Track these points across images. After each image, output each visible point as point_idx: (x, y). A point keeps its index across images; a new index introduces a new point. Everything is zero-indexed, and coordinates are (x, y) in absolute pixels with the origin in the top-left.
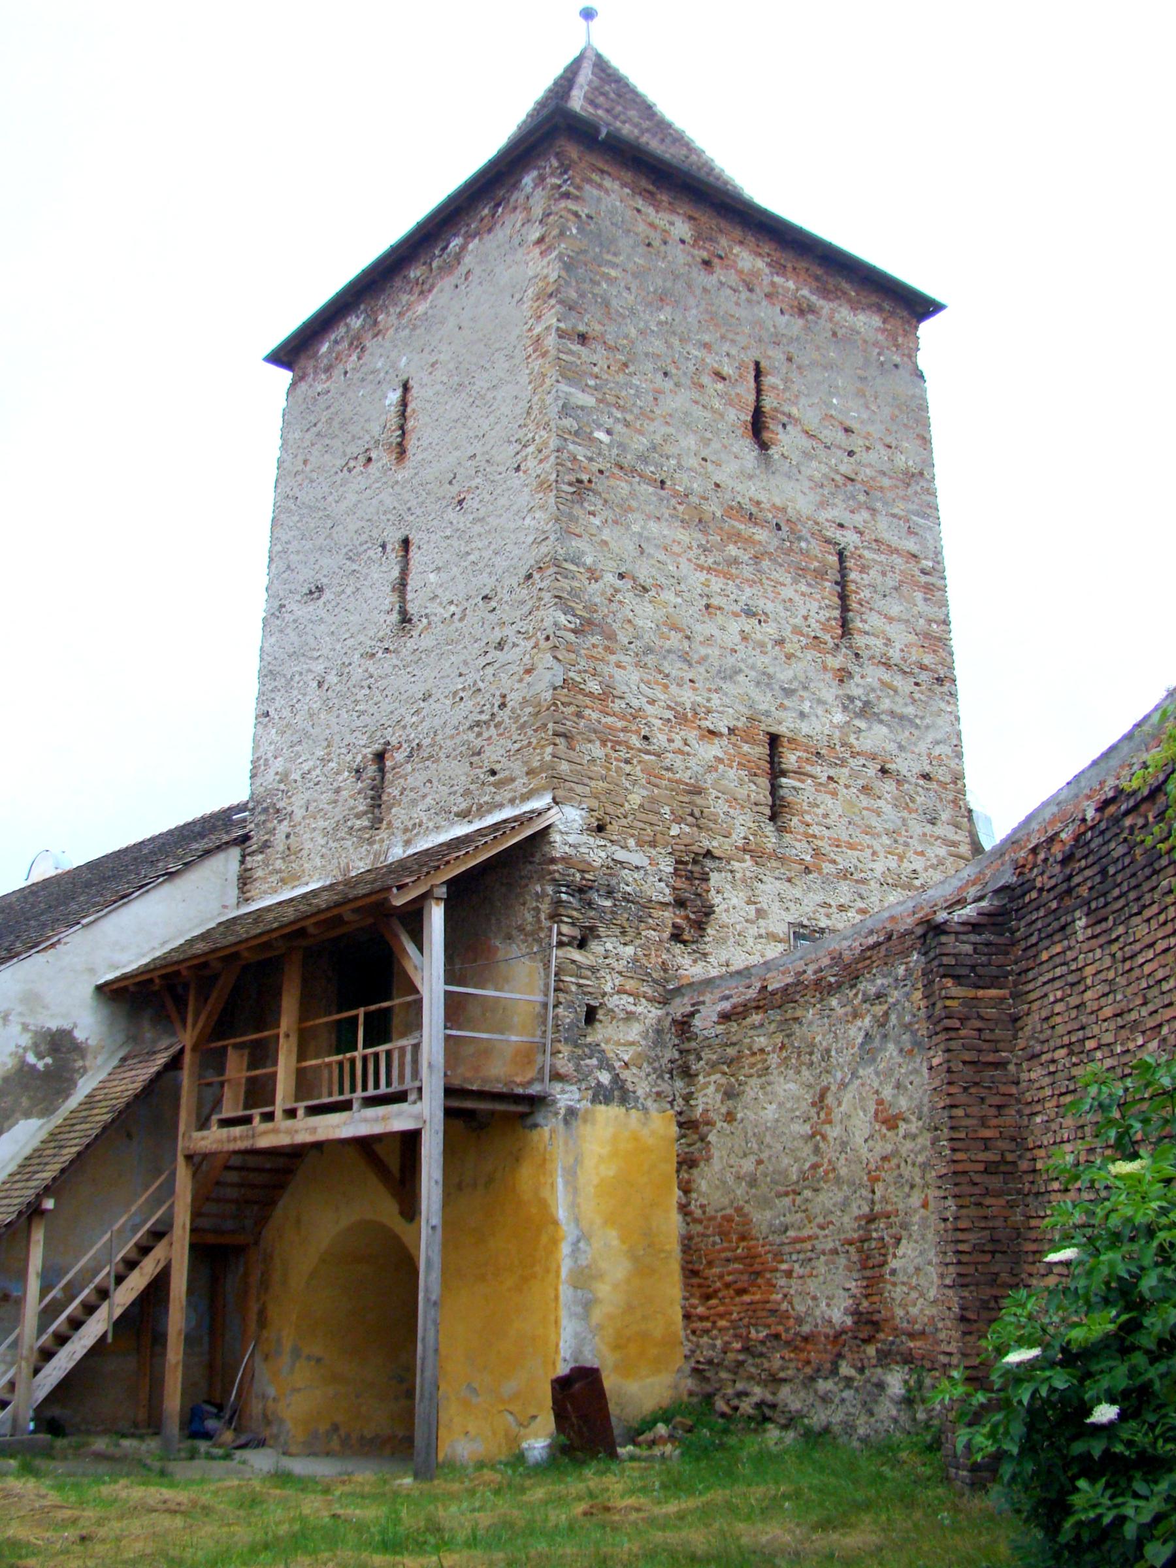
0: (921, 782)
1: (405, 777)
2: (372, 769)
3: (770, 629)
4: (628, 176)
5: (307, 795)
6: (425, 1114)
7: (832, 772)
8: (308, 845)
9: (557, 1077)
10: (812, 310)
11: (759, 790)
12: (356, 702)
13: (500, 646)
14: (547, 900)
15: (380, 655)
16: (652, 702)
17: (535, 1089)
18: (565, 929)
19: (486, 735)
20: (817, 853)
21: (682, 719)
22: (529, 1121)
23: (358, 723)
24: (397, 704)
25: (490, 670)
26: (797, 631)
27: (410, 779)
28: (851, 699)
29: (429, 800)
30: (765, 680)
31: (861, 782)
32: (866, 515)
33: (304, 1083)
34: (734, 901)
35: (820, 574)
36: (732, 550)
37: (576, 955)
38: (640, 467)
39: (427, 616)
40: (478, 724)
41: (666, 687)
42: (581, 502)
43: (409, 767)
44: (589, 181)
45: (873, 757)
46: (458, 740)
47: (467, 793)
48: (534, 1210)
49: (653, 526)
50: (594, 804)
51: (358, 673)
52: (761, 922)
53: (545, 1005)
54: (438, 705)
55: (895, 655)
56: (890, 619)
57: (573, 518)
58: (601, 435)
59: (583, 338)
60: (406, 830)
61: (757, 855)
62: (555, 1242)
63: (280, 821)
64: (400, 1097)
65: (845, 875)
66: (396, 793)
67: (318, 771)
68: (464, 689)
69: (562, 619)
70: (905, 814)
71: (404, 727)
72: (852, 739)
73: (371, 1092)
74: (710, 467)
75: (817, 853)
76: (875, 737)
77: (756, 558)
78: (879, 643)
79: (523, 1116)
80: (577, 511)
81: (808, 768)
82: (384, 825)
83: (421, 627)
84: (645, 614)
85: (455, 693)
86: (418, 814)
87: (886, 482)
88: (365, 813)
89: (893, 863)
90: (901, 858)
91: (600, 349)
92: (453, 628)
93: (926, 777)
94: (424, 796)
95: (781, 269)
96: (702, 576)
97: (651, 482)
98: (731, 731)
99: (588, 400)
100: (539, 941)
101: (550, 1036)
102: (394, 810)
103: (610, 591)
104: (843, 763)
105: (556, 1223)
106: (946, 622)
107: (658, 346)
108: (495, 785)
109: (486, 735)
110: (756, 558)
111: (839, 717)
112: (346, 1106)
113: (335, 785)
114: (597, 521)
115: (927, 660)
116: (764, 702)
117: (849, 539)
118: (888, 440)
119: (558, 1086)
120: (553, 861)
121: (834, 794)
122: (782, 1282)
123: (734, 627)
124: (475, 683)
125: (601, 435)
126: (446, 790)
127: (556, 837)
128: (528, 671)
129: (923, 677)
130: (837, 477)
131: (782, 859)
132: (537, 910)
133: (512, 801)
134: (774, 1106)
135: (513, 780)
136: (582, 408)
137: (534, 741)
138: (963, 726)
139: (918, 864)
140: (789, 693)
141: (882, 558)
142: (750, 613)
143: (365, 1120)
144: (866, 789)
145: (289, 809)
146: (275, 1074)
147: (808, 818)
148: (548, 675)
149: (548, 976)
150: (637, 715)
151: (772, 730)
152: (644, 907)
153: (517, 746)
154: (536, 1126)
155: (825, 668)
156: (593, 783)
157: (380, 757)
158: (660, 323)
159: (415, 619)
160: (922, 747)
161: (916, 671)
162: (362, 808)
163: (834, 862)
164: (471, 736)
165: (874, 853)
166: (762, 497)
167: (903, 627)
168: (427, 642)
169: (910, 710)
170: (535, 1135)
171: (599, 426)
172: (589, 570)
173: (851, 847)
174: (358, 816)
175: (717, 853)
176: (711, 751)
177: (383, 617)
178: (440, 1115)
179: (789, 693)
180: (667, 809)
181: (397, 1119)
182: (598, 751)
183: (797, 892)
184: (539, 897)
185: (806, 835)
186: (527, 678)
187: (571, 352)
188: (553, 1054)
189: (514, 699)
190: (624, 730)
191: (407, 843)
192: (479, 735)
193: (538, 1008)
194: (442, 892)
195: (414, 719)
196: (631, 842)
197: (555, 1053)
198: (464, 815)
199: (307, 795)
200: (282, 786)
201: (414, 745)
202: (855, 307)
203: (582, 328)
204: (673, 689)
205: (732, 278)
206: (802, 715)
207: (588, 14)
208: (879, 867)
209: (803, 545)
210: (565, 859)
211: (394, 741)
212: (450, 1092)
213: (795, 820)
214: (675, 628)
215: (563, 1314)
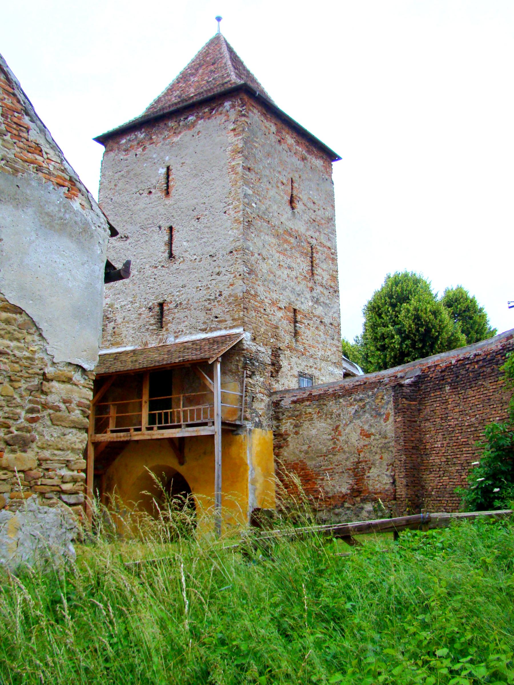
1: (174, 313)
2: (157, 309)
3: (294, 273)
4: (260, 108)
5: (124, 314)
6: (217, 429)
8: (125, 332)
9: (246, 419)
11: (290, 328)
12: (148, 283)
13: (218, 274)
14: (242, 362)
15: (160, 267)
16: (266, 298)
17: (238, 423)
18: (248, 372)
19: (213, 304)
20: (305, 349)
22: (235, 433)
23: (150, 291)
24: (169, 287)
25: (213, 282)
27: (177, 315)
28: (313, 297)
29: (186, 323)
30: (293, 291)
32: (318, 233)
33: (152, 420)
35: (306, 254)
36: (285, 246)
37: (250, 380)
38: (263, 216)
39: (182, 257)
40: (209, 300)
42: (250, 228)
43: (176, 310)
44: (250, 110)
46: (199, 304)
47: (204, 323)
48: (237, 461)
51: (149, 273)
53: (242, 396)
54: (189, 290)
55: (324, 282)
57: (248, 234)
58: (254, 205)
59: (249, 169)
60: (175, 332)
62: (246, 470)
63: (110, 322)
64: (205, 424)
65: (311, 356)
66: (170, 319)
67: (129, 306)
68: (201, 286)
69: (245, 269)
71: (173, 296)
73: (189, 422)
75: (305, 349)
78: (321, 278)
79: (233, 431)
82: (164, 329)
83: (180, 261)
85: (197, 288)
86: (181, 327)
87: (323, 222)
88: (155, 324)
91: (253, 173)
92: (196, 264)
94: (184, 322)
99: (250, 192)
100: (238, 375)
101: (243, 406)
102: (169, 325)
105: (247, 464)
106: (337, 272)
107: (267, 173)
108: (218, 322)
109: (213, 304)
111: (310, 304)
112: (179, 426)
113: (139, 312)
114: (253, 235)
117: (314, 242)
118: (324, 207)
119: (246, 422)
120: (244, 350)
121: (309, 329)
122: (320, 482)
124: (207, 285)
125: (254, 205)
126: (195, 321)
127: (244, 342)
128: (231, 285)
129: (331, 290)
132: (238, 365)
133: (225, 328)
134: (315, 430)
135: (226, 321)
136: (249, 195)
137: (235, 310)
138: (341, 307)
139: (329, 354)
142: (290, 268)
143: (188, 431)
145: (114, 318)
146: (141, 415)
148: (241, 288)
149: (243, 387)
153: (227, 310)
154: (238, 434)
156: (253, 325)
157: (161, 305)
158: (268, 164)
159: (177, 257)
162: (152, 322)
164: (206, 304)
168: (183, 266)
169: (328, 302)
170: (238, 437)
173: (313, 347)
174: (151, 325)
175: (281, 348)
176: (280, 314)
177: (160, 254)
178: (220, 430)
180: (270, 334)
181: (204, 431)
182: (254, 314)
183: (300, 362)
184: (237, 361)
186: (231, 287)
187: (246, 175)
188: (245, 412)
189: (225, 294)
191: (176, 337)
192: (209, 304)
193: (238, 397)
194: (220, 359)
195: (178, 293)
197: (245, 412)
198: (204, 330)
199: (124, 314)
200: (110, 309)
201: (178, 303)
203: (249, 166)
206: (302, 303)
207: (219, 19)
210: (247, 349)
211: (168, 300)
212: (223, 423)
215: (249, 492)
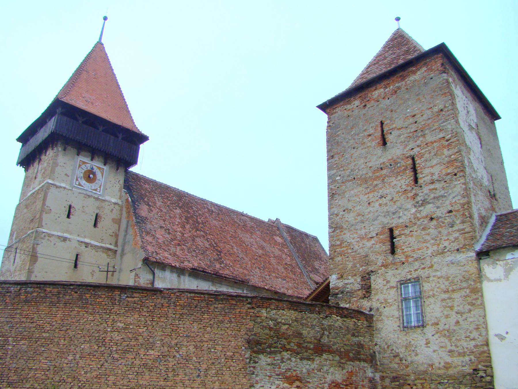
0: (447, 215)
7: (411, 229)
10: (399, 88)
11: (388, 247)
21: (362, 238)
26: (398, 192)
28: (417, 202)
30: (387, 214)
31: (421, 227)
34: (380, 281)
36: (375, 183)
41: (357, 232)
49: (352, 192)
50: (339, 272)
52: (388, 284)
55: (436, 177)
56: (432, 167)
61: (385, 266)
65: (416, 260)
70: (440, 229)
72: (418, 215)
74: (367, 164)
75: (407, 257)
76: (428, 209)
80: (333, 202)
81: (403, 232)
84: (350, 217)
87: (430, 121)
89: (435, 248)
90: (438, 245)
93: (451, 211)
95: (386, 88)
96: (367, 196)
97: (351, 181)
98: (377, 234)
103: (341, 217)
104: (415, 224)
111: (413, 210)
114: (337, 201)
115: (449, 171)
116: (386, 220)
118: (430, 106)
121: (412, 236)
123: (377, 204)
125: (338, 178)
129: (449, 177)
130: (411, 135)
131: (394, 264)
139: (446, 244)
140: (394, 213)
141: (429, 148)
142: (382, 197)
144: (424, 229)
147: (403, 248)
150: (350, 244)
151: (390, 227)
152: (351, 293)
155: (408, 198)
160: (448, 202)
161: (444, 177)
163: (413, 257)
165: (428, 248)
166: (385, 160)
167: (439, 165)
171: (337, 176)
172: (336, 214)
173: (419, 249)
175: (373, 270)
176: (369, 244)
179: (394, 213)
180: (358, 265)
182: (340, 258)
185: (403, 253)
190: (347, 249)
196: (350, 277)
202: (414, 73)
204: (359, 232)
208: (429, 252)
209: (399, 165)
213: (399, 250)
214: (359, 215)
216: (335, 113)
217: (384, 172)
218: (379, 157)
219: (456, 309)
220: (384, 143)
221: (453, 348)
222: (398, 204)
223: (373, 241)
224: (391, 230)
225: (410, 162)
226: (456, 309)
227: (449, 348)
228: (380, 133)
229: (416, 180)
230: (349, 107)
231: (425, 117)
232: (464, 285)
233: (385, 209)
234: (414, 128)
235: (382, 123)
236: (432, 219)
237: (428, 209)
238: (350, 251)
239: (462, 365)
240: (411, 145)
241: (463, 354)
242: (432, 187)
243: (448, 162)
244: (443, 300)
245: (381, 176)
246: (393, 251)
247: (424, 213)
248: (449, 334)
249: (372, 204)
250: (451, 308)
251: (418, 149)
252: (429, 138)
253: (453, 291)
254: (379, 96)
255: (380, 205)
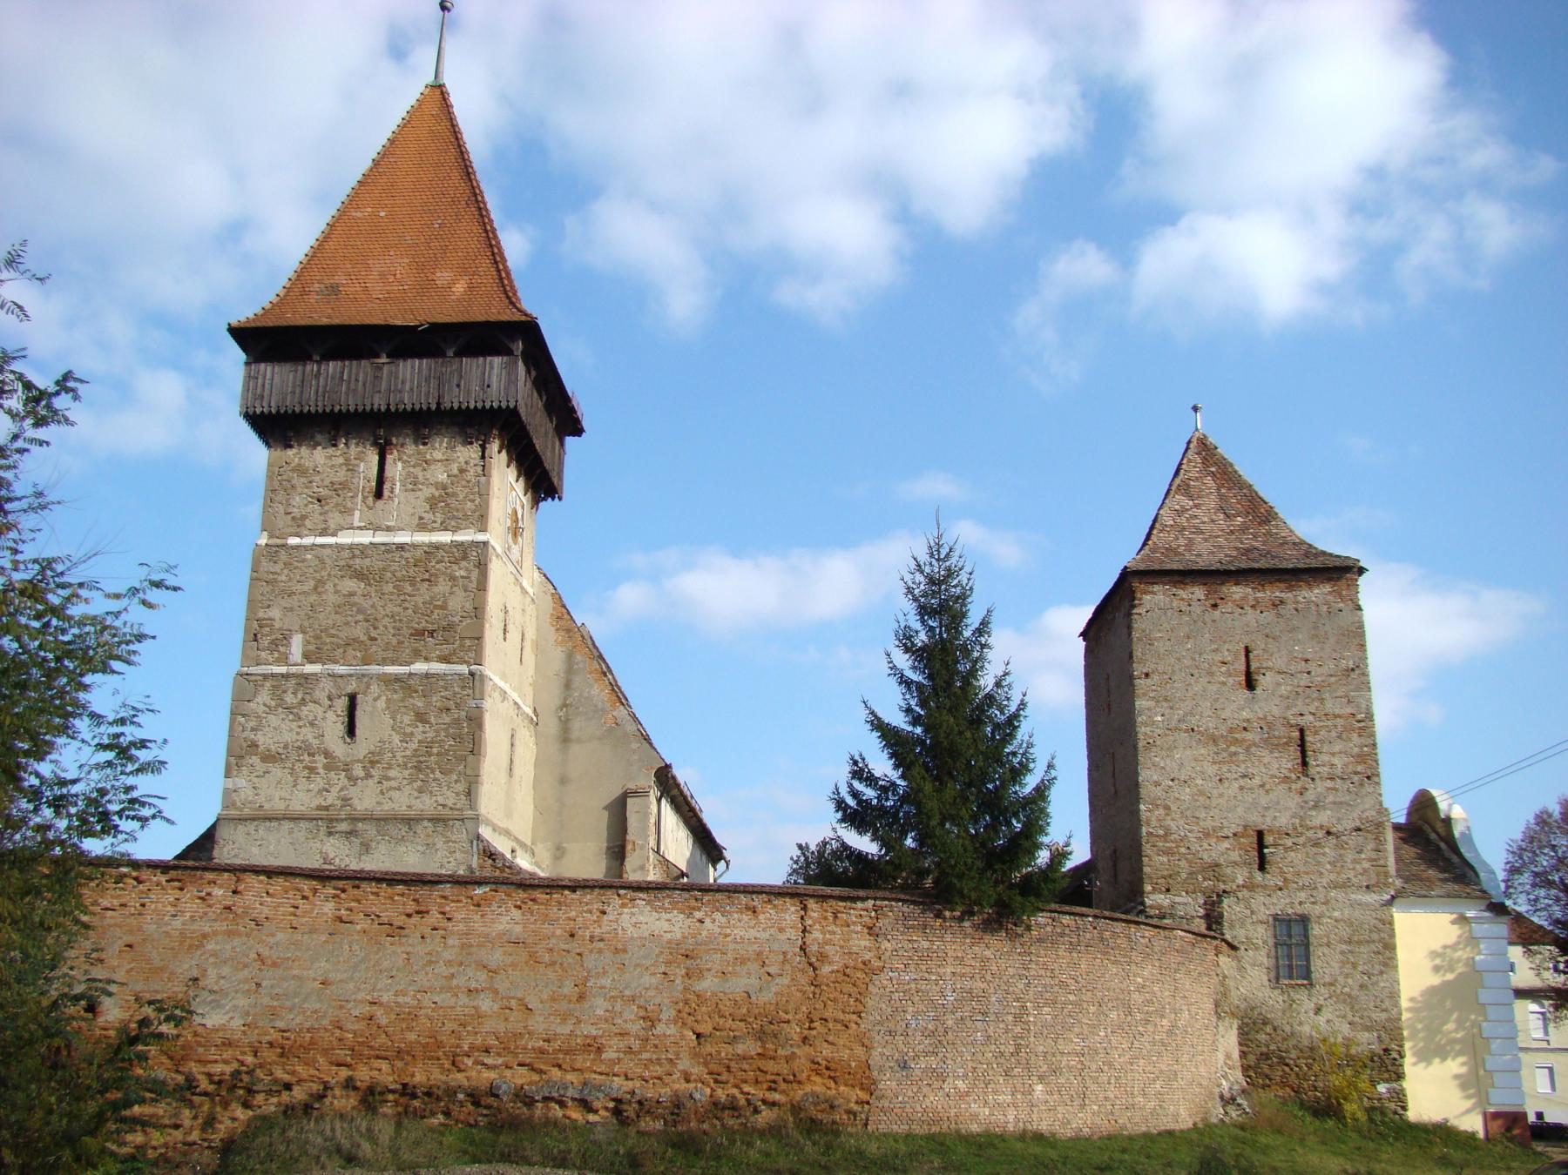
3: (1257, 781)
20: (1285, 880)
21: (1207, 835)
26: (1273, 776)
36: (1233, 749)
45: (1321, 827)
55: (1338, 771)
56: (1333, 754)
65: (1303, 888)
75: (1285, 880)
77: (1248, 749)
87: (1333, 679)
89: (1333, 877)
97: (1186, 731)
106: (1374, 745)
110: (1248, 749)
115: (1360, 768)
139: (1351, 874)
142: (1244, 776)
205: (1229, 607)
216: (1154, 593)
217: (1249, 736)
218: (1238, 706)
219: (1360, 968)
220: (1250, 684)
221: (1357, 1019)
222: (1272, 796)
223: (1226, 844)
224: (1260, 834)
225: (1296, 734)
226: (1360, 968)
227: (1350, 1018)
228: (1243, 668)
229: (1305, 764)
230: (1180, 592)
231: (1324, 670)
232: (1375, 936)
233: (1249, 798)
234: (1304, 680)
235: (1247, 651)
236: (1329, 833)
237: (1322, 818)
238: (1183, 850)
239: (1366, 1042)
240: (1300, 707)
241: (1367, 1029)
242: (1329, 784)
243: (1359, 756)
244: (1342, 953)
245: (1244, 740)
246: (1262, 868)
247: (1316, 822)
248: (1350, 1000)
249: (1226, 784)
250: (1354, 966)
251: (1311, 718)
252: (1330, 706)
253: (1359, 943)
254: (1242, 599)
255: (1241, 788)
